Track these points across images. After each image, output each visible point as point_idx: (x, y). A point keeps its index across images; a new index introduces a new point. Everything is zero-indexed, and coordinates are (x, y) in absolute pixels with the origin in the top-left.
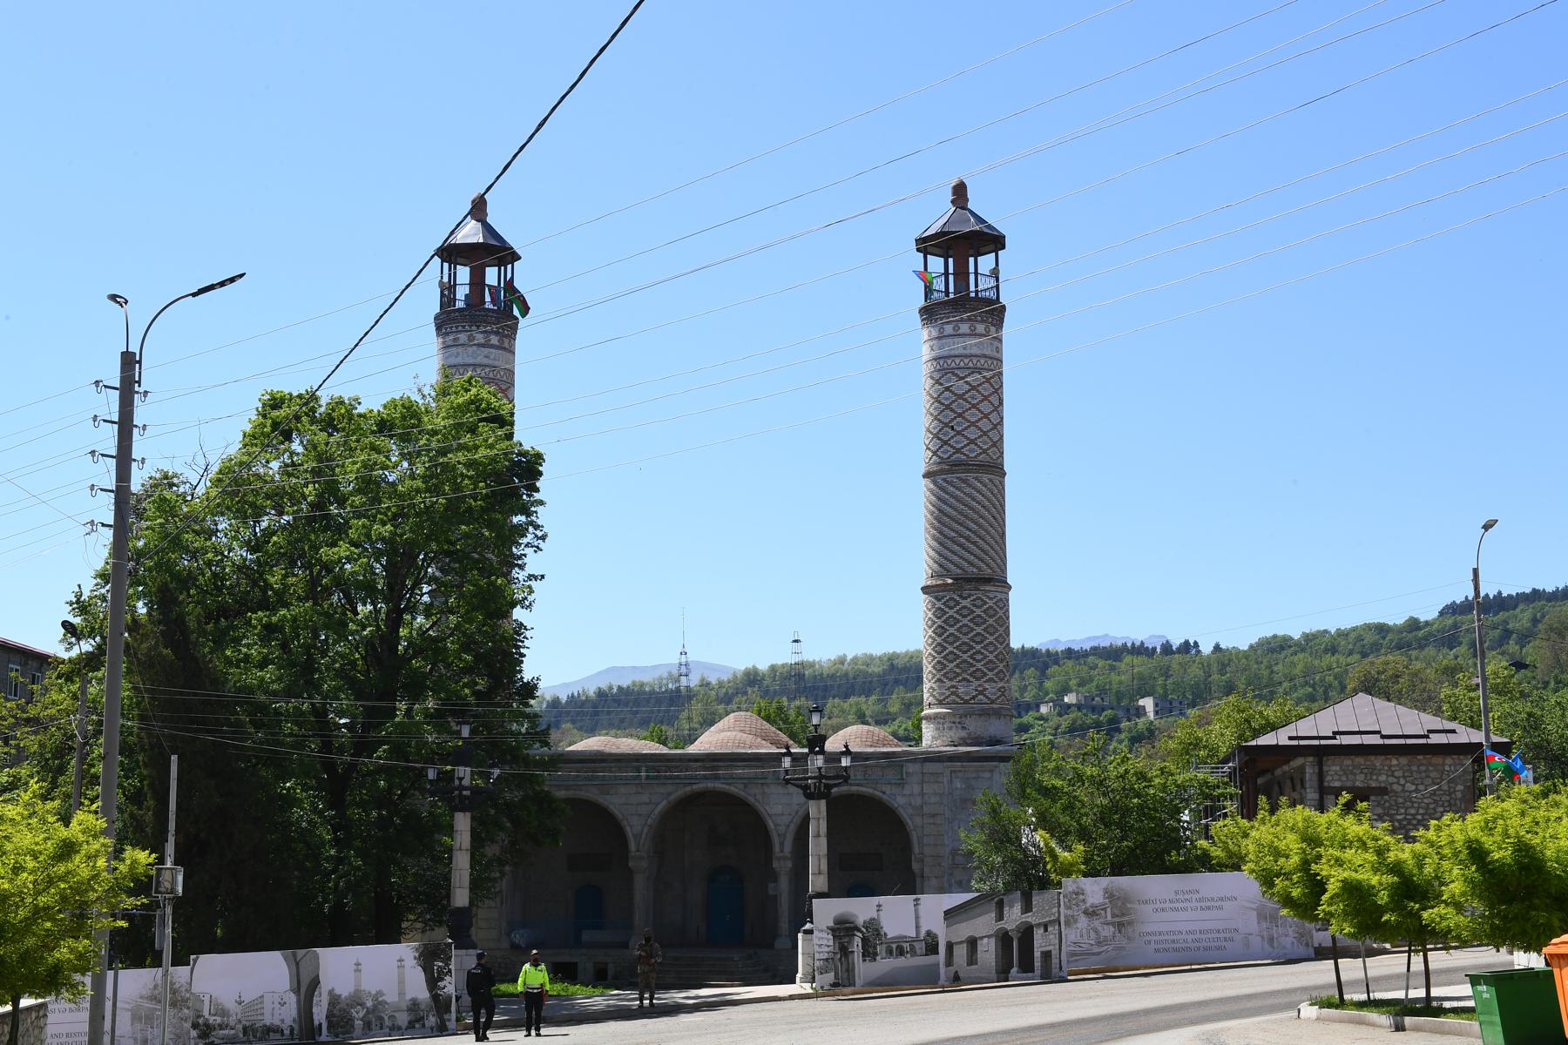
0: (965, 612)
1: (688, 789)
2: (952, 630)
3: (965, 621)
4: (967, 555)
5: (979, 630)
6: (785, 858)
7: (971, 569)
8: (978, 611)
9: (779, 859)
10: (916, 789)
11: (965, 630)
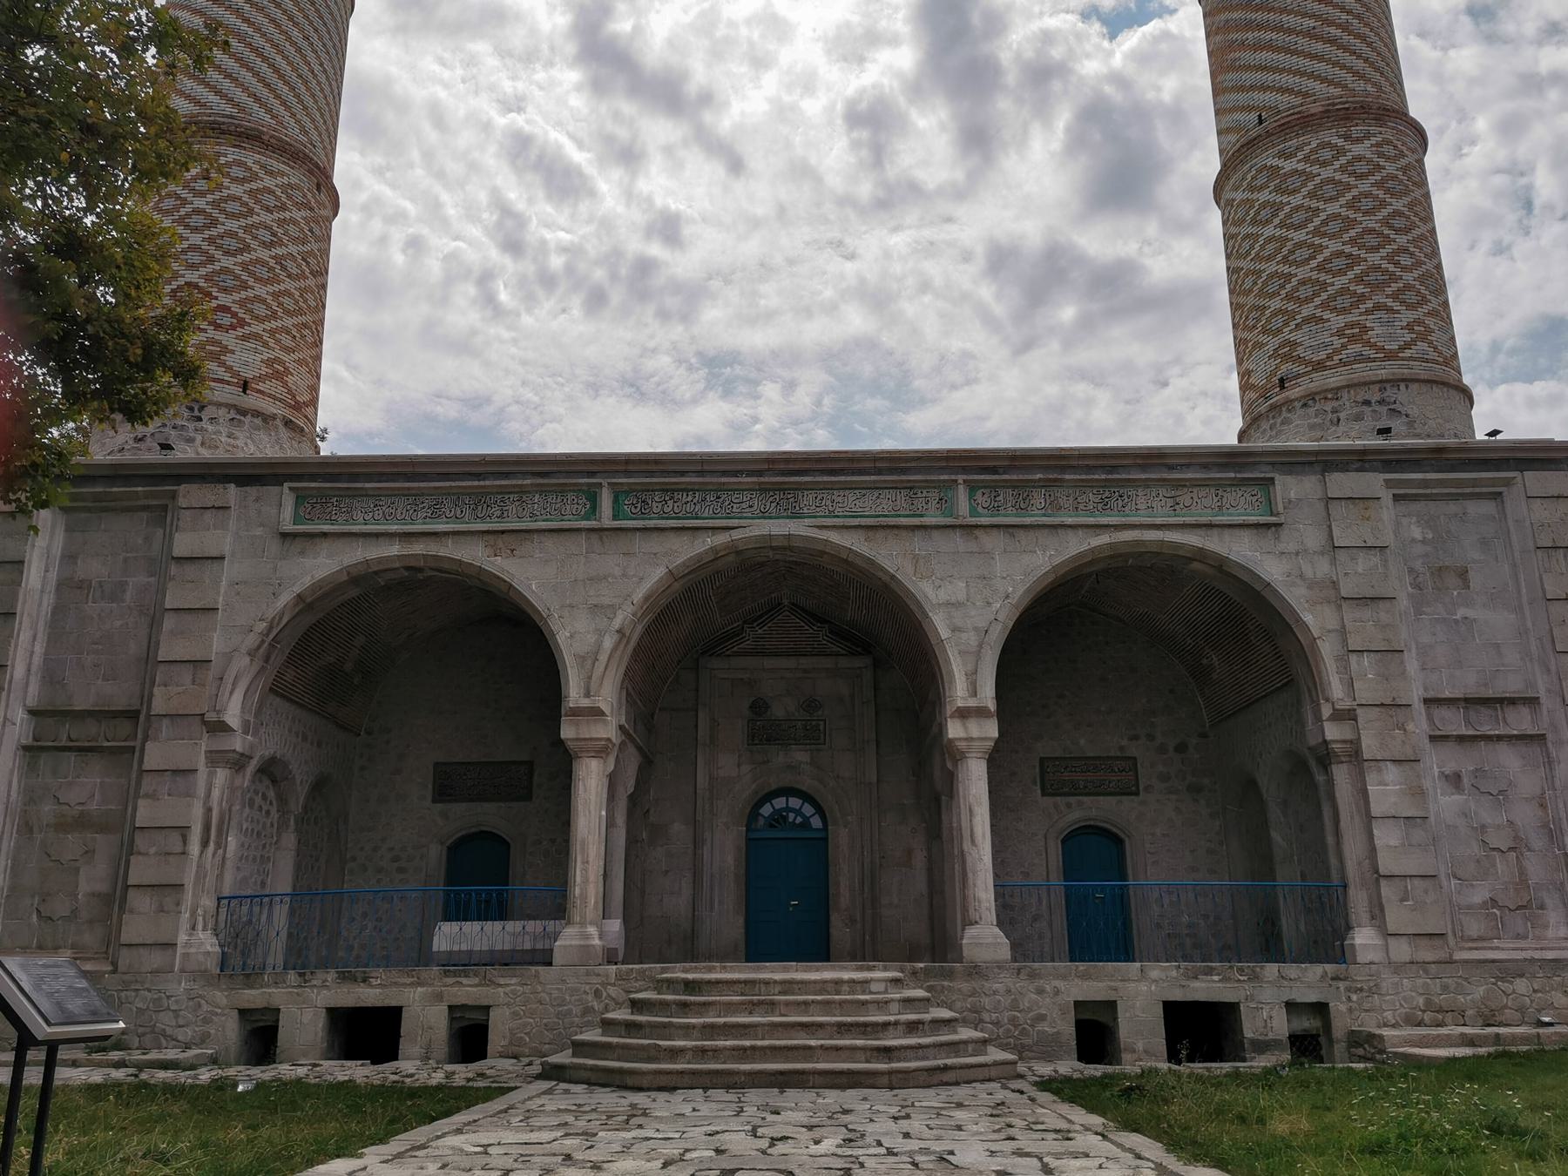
0: (1362, 168)
1: (721, 539)
2: (1333, 208)
3: (1364, 186)
4: (1349, 59)
5: (1398, 204)
6: (981, 712)
7: (1360, 86)
8: (1390, 168)
9: (964, 714)
10: (1313, 538)
11: (1366, 204)
